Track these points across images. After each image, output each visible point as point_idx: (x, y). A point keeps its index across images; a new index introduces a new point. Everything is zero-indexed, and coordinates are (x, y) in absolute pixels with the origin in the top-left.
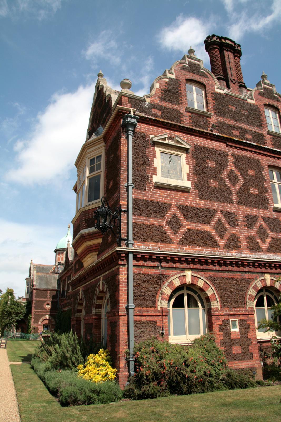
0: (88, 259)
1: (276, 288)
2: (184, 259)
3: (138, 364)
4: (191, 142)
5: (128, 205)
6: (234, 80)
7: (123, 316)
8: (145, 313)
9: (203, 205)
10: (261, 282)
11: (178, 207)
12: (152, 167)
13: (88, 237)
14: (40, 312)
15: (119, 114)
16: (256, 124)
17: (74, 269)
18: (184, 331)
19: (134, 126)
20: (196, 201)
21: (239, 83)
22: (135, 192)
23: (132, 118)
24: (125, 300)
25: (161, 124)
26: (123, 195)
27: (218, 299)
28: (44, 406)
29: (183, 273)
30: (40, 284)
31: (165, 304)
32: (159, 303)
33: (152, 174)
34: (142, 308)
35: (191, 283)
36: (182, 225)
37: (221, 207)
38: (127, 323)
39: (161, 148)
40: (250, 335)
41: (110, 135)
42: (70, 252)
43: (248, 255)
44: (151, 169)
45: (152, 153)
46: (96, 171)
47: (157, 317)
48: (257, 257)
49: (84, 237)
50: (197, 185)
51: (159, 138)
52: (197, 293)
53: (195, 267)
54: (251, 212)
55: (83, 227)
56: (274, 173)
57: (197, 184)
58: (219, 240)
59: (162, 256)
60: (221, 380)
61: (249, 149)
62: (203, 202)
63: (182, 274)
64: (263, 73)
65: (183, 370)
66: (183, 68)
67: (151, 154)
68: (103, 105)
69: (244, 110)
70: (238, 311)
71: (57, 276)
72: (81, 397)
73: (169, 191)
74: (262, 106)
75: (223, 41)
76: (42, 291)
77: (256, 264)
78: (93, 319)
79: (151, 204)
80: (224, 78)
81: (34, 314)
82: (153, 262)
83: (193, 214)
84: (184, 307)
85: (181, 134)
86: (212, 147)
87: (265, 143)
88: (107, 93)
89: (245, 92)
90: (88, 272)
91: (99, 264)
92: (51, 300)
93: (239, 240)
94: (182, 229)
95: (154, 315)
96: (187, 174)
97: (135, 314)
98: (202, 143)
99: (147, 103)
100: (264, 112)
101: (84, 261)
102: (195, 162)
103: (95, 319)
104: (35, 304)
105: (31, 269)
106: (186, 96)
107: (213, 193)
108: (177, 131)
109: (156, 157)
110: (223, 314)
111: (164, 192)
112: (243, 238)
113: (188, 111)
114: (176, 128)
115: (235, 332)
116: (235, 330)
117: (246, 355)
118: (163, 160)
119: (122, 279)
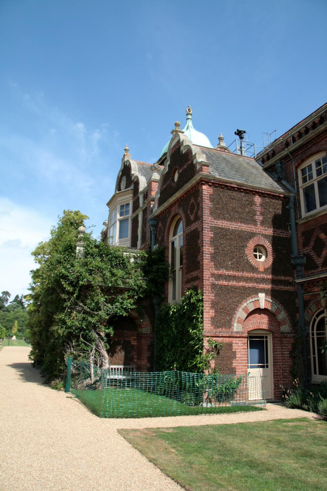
14: (234, 278)
81: (213, 286)
104: (213, 242)
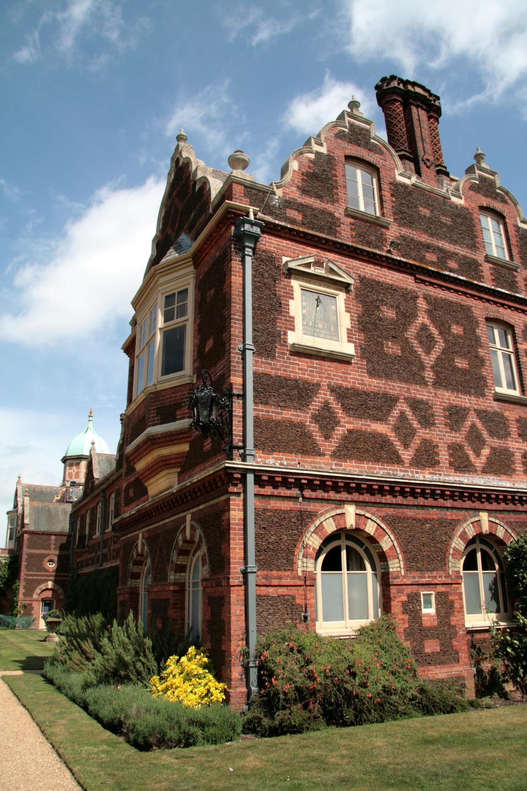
0: (158, 480)
1: (498, 537)
2: (343, 484)
3: (266, 672)
4: (354, 273)
5: (244, 385)
6: (428, 160)
7: (237, 586)
8: (275, 582)
9: (374, 386)
10: (473, 526)
11: (332, 390)
12: (286, 316)
13: (161, 440)
14: (36, 575)
15: (229, 216)
16: (465, 242)
17: (125, 498)
18: (342, 613)
19: (255, 238)
20: (362, 380)
21: (437, 166)
22: (257, 362)
23: (252, 224)
24: (239, 558)
25: (301, 237)
26: (235, 366)
27: (400, 556)
28: (107, 752)
29: (340, 508)
30: (36, 523)
31: (309, 565)
32: (300, 563)
33: (286, 328)
34: (269, 573)
35: (354, 527)
36: (339, 422)
37: (406, 392)
38: (243, 598)
39: (303, 281)
40: (454, 620)
41: (207, 254)
42: (96, 462)
43: (451, 479)
44: (285, 320)
45: (286, 289)
46: (177, 318)
47: (295, 588)
48: (466, 481)
49: (155, 439)
50: (364, 351)
51: (300, 262)
52: (364, 544)
53: (361, 498)
54: (458, 401)
55: (152, 421)
56: (496, 332)
57: (364, 349)
58: (402, 450)
59: (305, 479)
60: (410, 700)
61: (453, 287)
62: (375, 381)
63: (339, 511)
64: (478, 150)
65: (347, 682)
66: (340, 136)
67: (284, 292)
68: (189, 195)
69: (446, 216)
70: (435, 577)
71: (69, 508)
72: (173, 734)
73: (316, 359)
74: (477, 210)
75: (410, 88)
76: (42, 536)
77: (465, 494)
78: (169, 590)
79: (284, 383)
80: (412, 157)
81: (25, 579)
82: (289, 488)
83: (358, 402)
84: (341, 570)
85: (337, 256)
86: (391, 282)
87: (480, 278)
88: (200, 175)
89: (447, 184)
90: (157, 505)
91: (184, 491)
92: (57, 552)
93: (436, 450)
94: (338, 430)
95: (291, 584)
96: (348, 329)
97: (259, 584)
98: (372, 275)
99: (277, 197)
100: (480, 220)
101: (150, 484)
102: (360, 309)
103: (174, 591)
104: (27, 560)
105: (19, 494)
106: (345, 187)
107: (391, 365)
108: (330, 251)
109: (292, 298)
110: (410, 583)
111: (307, 362)
112: (442, 447)
113: (348, 214)
114: (329, 246)
115: (429, 615)
116: (429, 611)
117: (448, 656)
118: (304, 303)
119: (235, 519)
